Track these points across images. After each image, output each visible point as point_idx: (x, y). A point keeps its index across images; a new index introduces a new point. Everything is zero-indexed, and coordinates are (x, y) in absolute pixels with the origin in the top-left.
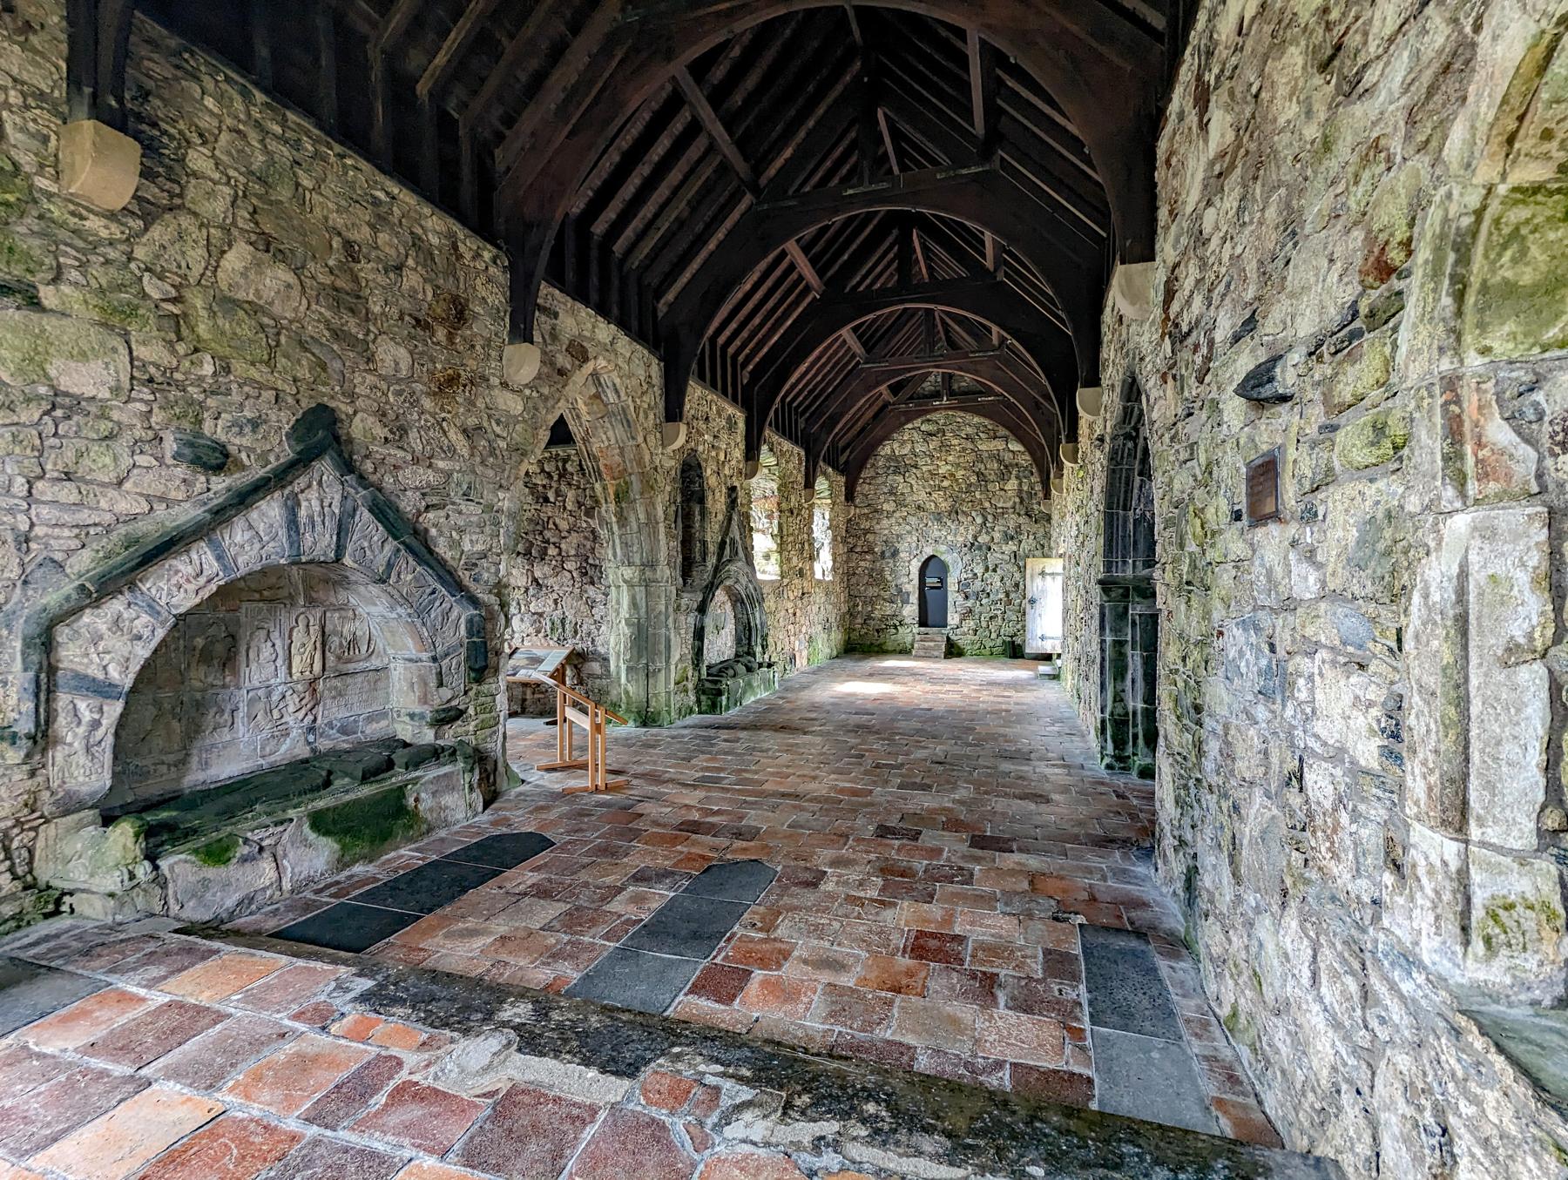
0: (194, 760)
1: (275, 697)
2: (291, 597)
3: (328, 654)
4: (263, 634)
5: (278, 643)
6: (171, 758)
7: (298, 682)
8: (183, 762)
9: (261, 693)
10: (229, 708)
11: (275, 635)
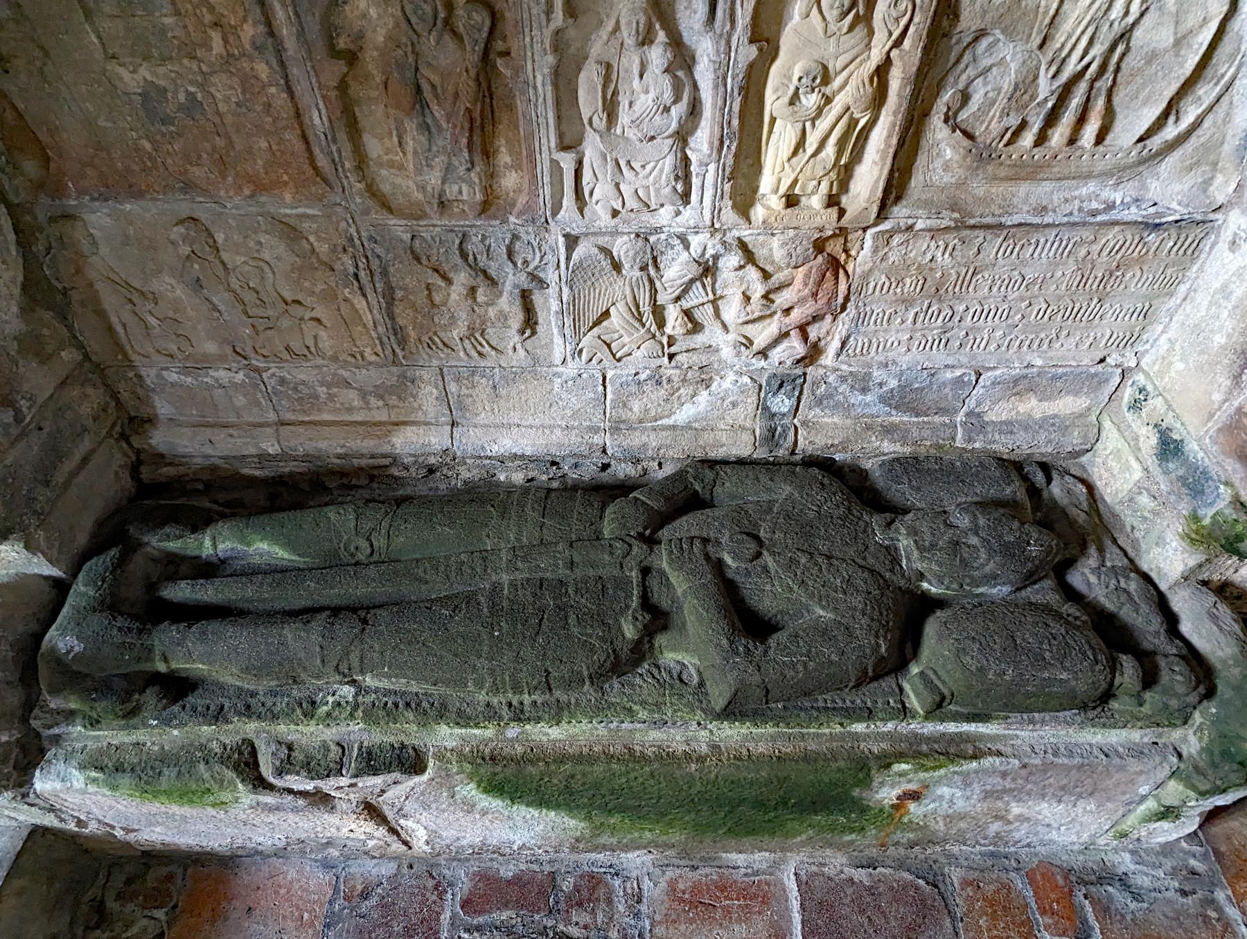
0: (428, 397)
1: (676, 269)
3: (937, 131)
5: (705, 49)
6: (368, 376)
8: (403, 387)
9: (622, 247)
10: (512, 280)
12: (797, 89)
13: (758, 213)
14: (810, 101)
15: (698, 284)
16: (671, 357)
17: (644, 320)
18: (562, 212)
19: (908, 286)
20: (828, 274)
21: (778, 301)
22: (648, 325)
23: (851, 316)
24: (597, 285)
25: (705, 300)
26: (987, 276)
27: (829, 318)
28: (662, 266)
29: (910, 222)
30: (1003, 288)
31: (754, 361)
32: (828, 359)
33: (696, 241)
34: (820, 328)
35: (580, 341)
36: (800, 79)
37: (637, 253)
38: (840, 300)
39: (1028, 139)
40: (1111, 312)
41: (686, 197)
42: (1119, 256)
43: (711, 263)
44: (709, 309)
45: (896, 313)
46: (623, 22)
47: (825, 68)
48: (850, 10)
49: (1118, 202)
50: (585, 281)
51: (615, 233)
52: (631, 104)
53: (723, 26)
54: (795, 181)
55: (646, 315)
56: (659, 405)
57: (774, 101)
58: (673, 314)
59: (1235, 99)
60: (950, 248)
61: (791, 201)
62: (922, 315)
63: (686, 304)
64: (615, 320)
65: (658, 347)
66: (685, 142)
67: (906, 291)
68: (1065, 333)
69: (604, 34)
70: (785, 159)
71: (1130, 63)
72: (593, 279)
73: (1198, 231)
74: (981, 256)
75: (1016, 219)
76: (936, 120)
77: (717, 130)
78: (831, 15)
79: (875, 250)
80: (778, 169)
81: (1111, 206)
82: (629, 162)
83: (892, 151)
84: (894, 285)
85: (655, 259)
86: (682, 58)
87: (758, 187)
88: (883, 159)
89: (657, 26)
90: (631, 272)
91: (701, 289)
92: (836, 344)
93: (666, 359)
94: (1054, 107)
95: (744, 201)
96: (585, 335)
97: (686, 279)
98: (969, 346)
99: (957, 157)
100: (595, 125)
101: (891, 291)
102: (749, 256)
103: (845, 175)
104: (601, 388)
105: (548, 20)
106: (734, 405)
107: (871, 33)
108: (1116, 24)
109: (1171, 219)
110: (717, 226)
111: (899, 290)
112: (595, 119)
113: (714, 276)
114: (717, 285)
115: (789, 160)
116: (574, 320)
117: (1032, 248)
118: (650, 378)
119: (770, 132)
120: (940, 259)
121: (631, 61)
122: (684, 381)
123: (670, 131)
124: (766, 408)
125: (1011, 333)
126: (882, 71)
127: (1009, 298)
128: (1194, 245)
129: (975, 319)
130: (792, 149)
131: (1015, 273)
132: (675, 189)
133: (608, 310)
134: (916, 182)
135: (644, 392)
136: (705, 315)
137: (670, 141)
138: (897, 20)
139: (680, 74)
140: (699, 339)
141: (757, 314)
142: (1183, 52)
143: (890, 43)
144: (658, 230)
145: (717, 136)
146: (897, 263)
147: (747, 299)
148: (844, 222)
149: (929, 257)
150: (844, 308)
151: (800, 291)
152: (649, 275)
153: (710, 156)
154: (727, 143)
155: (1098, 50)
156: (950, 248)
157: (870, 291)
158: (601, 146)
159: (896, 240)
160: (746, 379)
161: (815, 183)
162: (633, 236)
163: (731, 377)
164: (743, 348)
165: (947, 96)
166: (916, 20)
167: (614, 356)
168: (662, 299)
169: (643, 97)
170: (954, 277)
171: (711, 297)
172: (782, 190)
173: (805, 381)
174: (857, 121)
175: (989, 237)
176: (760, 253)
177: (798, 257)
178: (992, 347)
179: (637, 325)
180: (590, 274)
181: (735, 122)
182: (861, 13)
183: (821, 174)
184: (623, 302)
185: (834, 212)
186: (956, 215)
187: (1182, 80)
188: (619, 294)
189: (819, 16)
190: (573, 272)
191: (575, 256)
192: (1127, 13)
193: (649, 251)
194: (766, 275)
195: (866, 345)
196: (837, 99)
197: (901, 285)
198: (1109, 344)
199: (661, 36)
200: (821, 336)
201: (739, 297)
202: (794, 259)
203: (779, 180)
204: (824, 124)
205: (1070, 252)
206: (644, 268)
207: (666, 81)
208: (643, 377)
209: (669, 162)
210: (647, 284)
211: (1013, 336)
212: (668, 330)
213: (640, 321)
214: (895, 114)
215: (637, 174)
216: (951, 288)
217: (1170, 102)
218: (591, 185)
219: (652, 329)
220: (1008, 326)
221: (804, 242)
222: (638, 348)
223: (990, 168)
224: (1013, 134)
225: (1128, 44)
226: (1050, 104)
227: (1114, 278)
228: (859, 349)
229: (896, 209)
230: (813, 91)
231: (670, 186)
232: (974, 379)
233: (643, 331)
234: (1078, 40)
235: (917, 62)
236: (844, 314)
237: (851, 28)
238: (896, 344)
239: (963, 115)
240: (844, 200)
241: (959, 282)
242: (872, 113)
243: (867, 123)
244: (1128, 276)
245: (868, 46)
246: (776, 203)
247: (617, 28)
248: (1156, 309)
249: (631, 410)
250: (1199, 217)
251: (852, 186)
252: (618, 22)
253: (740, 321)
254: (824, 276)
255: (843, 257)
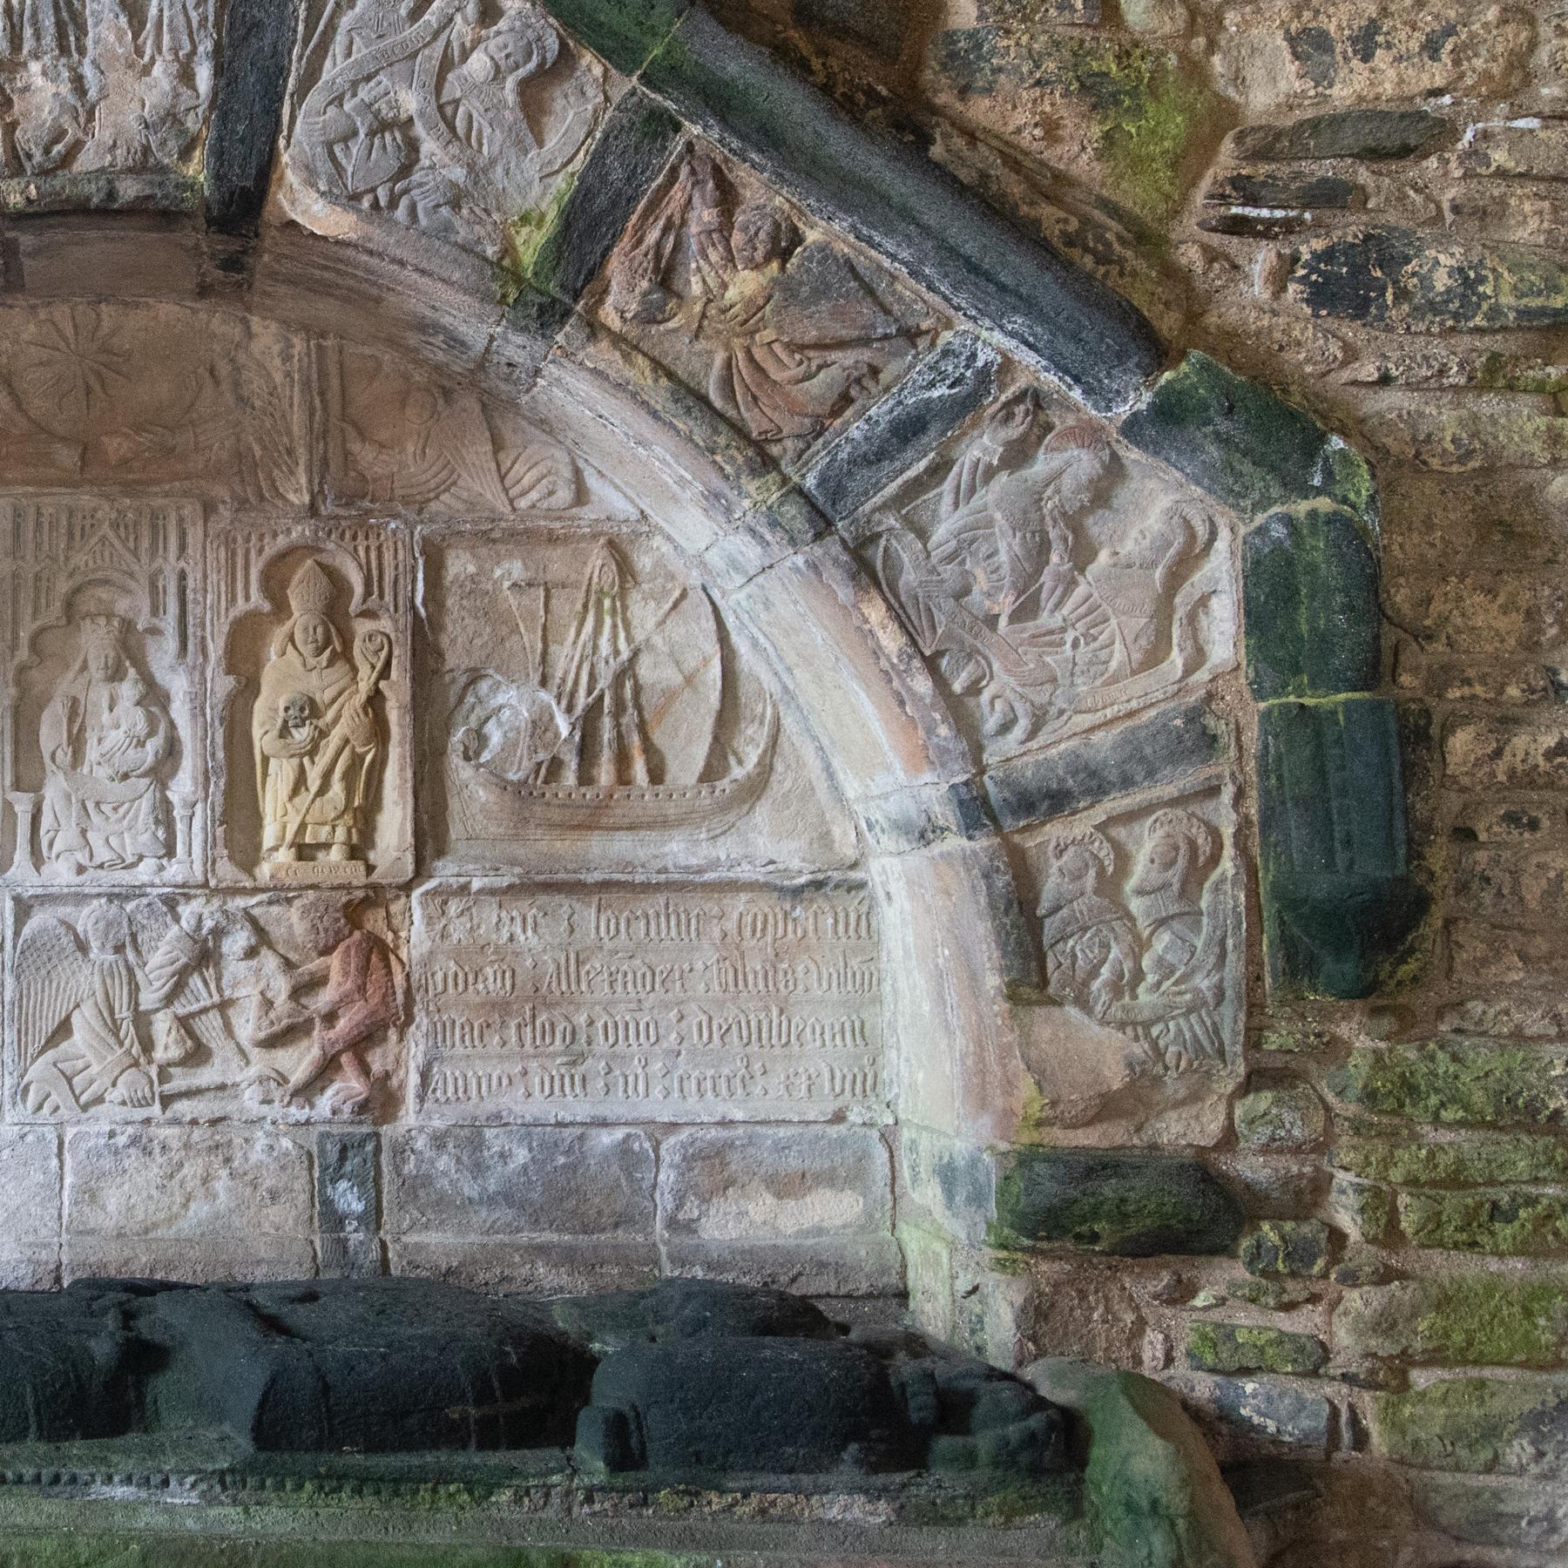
2: (242, 464)
3: (460, 771)
4: (95, 642)
5: (178, 685)
7: (281, 894)
9: (85, 919)
11: (162, 656)
12: (285, 722)
13: (264, 871)
14: (302, 735)
15: (196, 975)
16: (166, 1100)
17: (122, 1034)
18: (13, 869)
19: (491, 979)
20: (374, 958)
21: (312, 1008)
22: (127, 1042)
23: (424, 1029)
24: (54, 975)
25: (208, 1003)
26: (598, 966)
27: (393, 1035)
28: (144, 949)
29: (462, 880)
30: (630, 985)
31: (293, 1109)
32: (409, 1116)
33: (187, 911)
34: (384, 1056)
35: (26, 1070)
36: (287, 709)
37: (109, 925)
38: (400, 998)
39: (570, 777)
40: (808, 1030)
41: (170, 852)
42: (769, 938)
43: (211, 944)
44: (214, 1019)
45: (488, 1026)
46: (91, 657)
47: (312, 702)
48: (325, 649)
49: (723, 858)
50: (38, 969)
51: (80, 898)
52: (100, 740)
53: (196, 659)
54: (302, 827)
55: (124, 1026)
56: (150, 1197)
57: (262, 736)
58: (162, 1026)
59: (794, 738)
60: (530, 921)
61: (304, 852)
62: (529, 1029)
63: (180, 1009)
64: (78, 1036)
65: (144, 1081)
66: (164, 786)
67: (491, 988)
68: (757, 1066)
69: (71, 675)
70: (286, 799)
71: (649, 700)
72: (49, 967)
73: (852, 902)
74: (577, 935)
75: (597, 876)
76: (455, 760)
77: (199, 763)
78: (307, 650)
79: (430, 921)
80: (280, 812)
81: (715, 864)
82: (97, 804)
83: (409, 785)
84: (471, 978)
85: (134, 936)
86: (154, 697)
87: (260, 844)
88: (402, 796)
89: (128, 663)
90: (100, 954)
91: (200, 984)
92: (414, 1079)
93: (157, 1107)
94: (583, 738)
95: (247, 854)
96: (34, 1060)
97: (178, 965)
98: (621, 1089)
99: (492, 798)
100: (58, 760)
101: (471, 988)
102: (262, 938)
103: (365, 818)
104: (54, 1162)
105: (13, 656)
106: (274, 1196)
107: (354, 670)
108: (611, 660)
109: (802, 880)
110: (212, 883)
111: (480, 986)
112: (59, 754)
113: (217, 965)
114: (224, 982)
115: (291, 799)
116: (19, 1031)
117: (642, 923)
118: (134, 1141)
119: (265, 774)
120: (522, 938)
121: (101, 694)
122: (187, 1146)
123: (146, 766)
124: (327, 1203)
125: (676, 1066)
126: (375, 700)
127: (647, 1005)
128: (863, 923)
129: (611, 1040)
130: (291, 785)
131: (638, 962)
132: (154, 835)
133: (68, 1018)
134: (455, 831)
135: (125, 1171)
136: (209, 1027)
137: (147, 781)
138: (377, 652)
139: (153, 709)
140: (206, 1076)
141: (285, 1022)
142: (701, 689)
143: (375, 675)
144: (137, 891)
145: (201, 769)
146: (464, 943)
147: (268, 1004)
148: (375, 877)
149: (505, 935)
150: (410, 1019)
151: (340, 984)
152: (126, 961)
153: (194, 793)
154: (213, 779)
155: (603, 683)
156: (530, 921)
157: (440, 988)
158: (65, 784)
159: (454, 907)
160: (286, 1143)
161: (328, 828)
162: (103, 900)
163: (261, 1141)
164: (273, 1085)
165: (458, 735)
166: (396, 653)
167: (77, 1099)
168: (148, 999)
169: (113, 733)
170: (552, 968)
171: (216, 998)
172: (289, 836)
173: (378, 1150)
174: (362, 758)
175: (577, 906)
176: (277, 932)
177: (326, 930)
178: (657, 1092)
179: (112, 1040)
180: (45, 958)
181: (220, 755)
182: (339, 649)
183: (333, 815)
184: (91, 1002)
185: (360, 866)
186: (517, 870)
187: (714, 714)
188: (85, 988)
189: (295, 653)
190: (22, 952)
191: (26, 931)
192: (617, 652)
193: (125, 924)
194: (288, 965)
195: (460, 1083)
196: (333, 733)
197: (480, 979)
198: (838, 1090)
199: (132, 672)
200: (389, 1068)
201: (256, 998)
202: (322, 934)
203: (284, 827)
204: (323, 760)
205: (697, 929)
206: (119, 949)
207: (139, 713)
208: (122, 1140)
209: (145, 804)
210: (124, 972)
211: (681, 1072)
212: (159, 1055)
213: (116, 1034)
214: (401, 744)
215: (107, 818)
216: (554, 984)
217: (716, 738)
218: (52, 834)
219: (134, 1051)
220: (667, 1053)
221: (331, 909)
222: (114, 1084)
223: (538, 809)
224: (548, 771)
225: (636, 682)
226: (577, 738)
227: (781, 974)
228: (451, 1090)
229: (439, 864)
230: (303, 722)
231: (149, 834)
232: (647, 1145)
233: (120, 1052)
234: (578, 675)
235: (409, 692)
236: (413, 1027)
237: (330, 663)
238: (505, 1082)
239: (486, 756)
240: (372, 856)
241: (563, 976)
242: (377, 746)
243: (373, 761)
244: (800, 969)
245: (354, 680)
246: (285, 856)
247: (84, 667)
248: (873, 1028)
249: (103, 1208)
250: (837, 876)
251: (378, 840)
252: (85, 661)
253: (262, 1035)
254: (368, 960)
255: (390, 937)
